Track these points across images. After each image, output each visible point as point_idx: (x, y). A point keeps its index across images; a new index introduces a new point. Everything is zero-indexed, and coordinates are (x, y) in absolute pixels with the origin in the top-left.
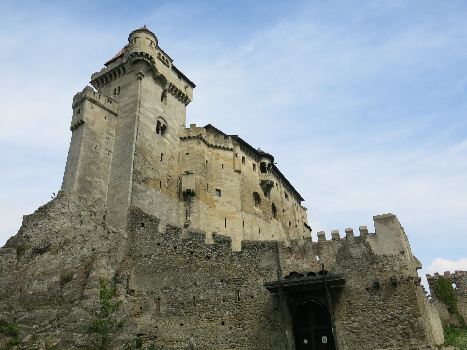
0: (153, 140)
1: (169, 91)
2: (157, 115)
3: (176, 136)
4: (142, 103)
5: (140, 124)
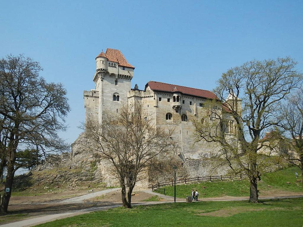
0: (111, 105)
1: (119, 78)
2: (113, 93)
3: (125, 98)
4: (104, 91)
5: (104, 101)
